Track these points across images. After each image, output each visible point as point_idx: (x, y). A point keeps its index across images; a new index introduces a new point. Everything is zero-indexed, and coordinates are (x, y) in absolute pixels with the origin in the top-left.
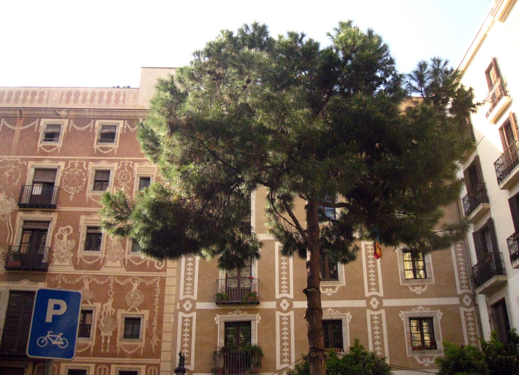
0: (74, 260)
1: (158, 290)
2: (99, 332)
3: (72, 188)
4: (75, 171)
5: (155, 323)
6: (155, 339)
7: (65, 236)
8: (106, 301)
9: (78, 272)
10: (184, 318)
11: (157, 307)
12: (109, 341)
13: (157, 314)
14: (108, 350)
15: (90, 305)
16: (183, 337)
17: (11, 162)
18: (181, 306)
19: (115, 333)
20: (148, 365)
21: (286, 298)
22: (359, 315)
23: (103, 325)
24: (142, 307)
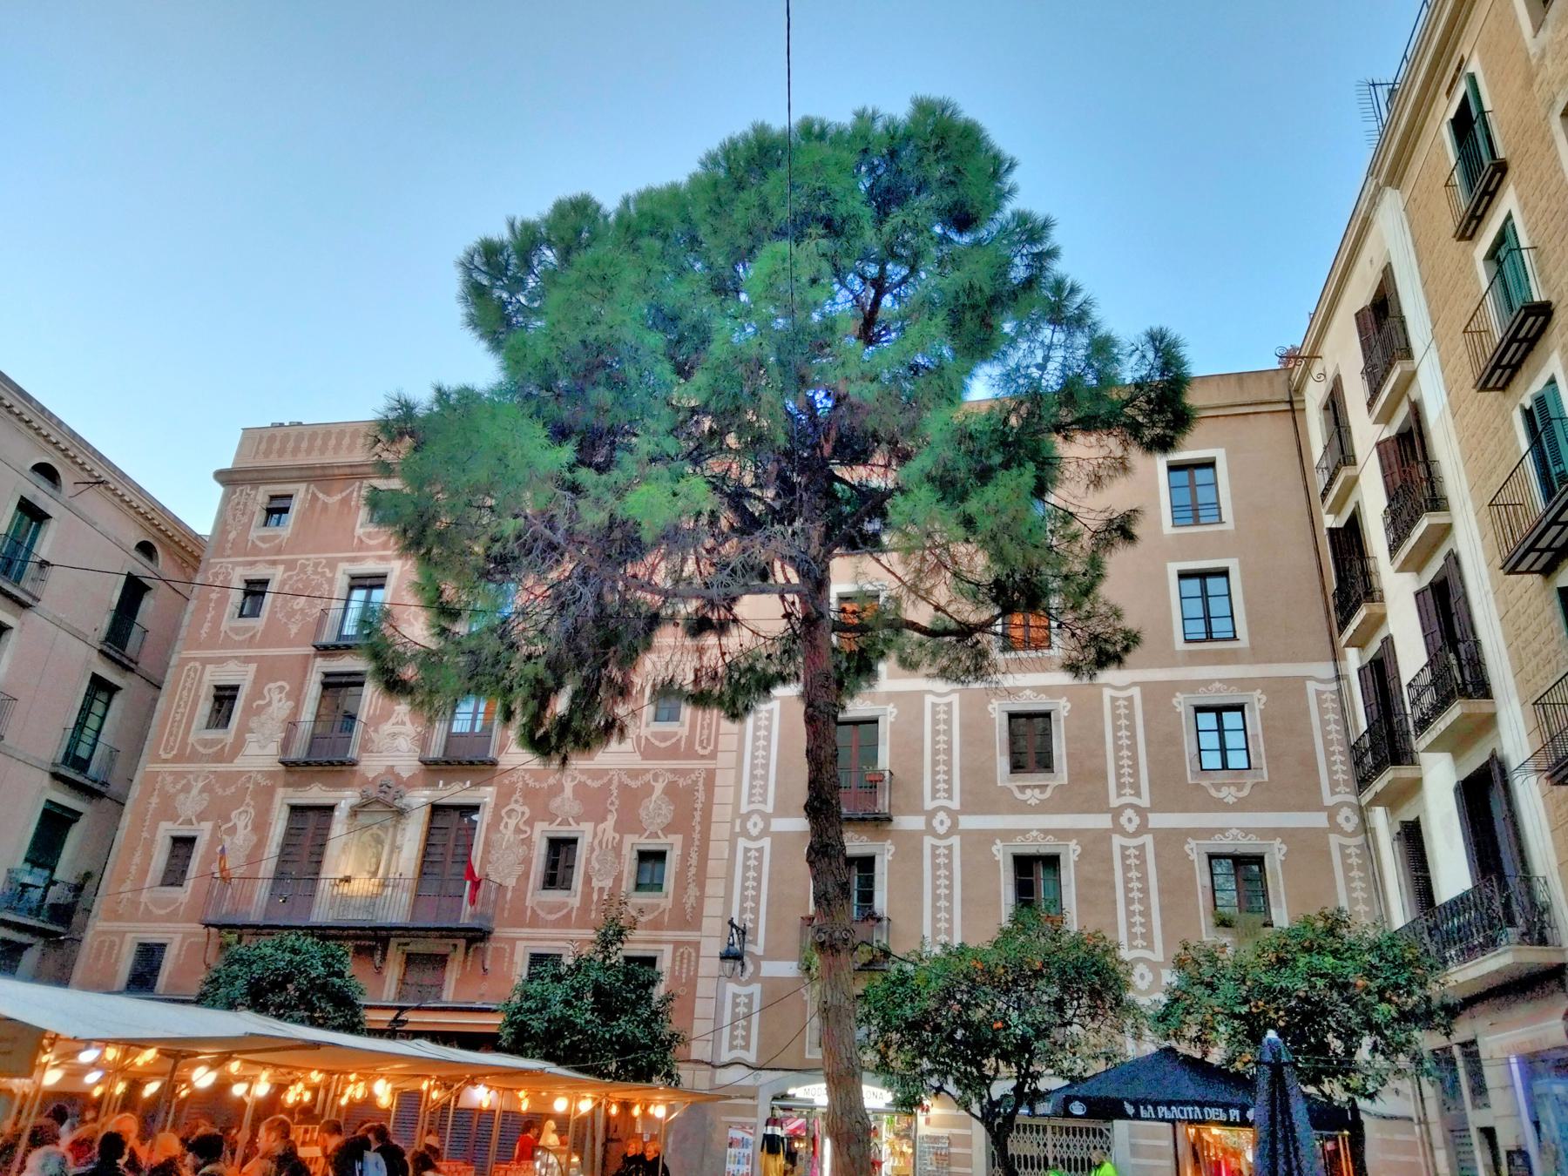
1: (701, 796)
2: (588, 880)
6: (693, 891)
8: (604, 819)
10: (747, 850)
11: (698, 828)
16: (744, 888)
19: (618, 880)
23: (597, 866)
24: (668, 829)
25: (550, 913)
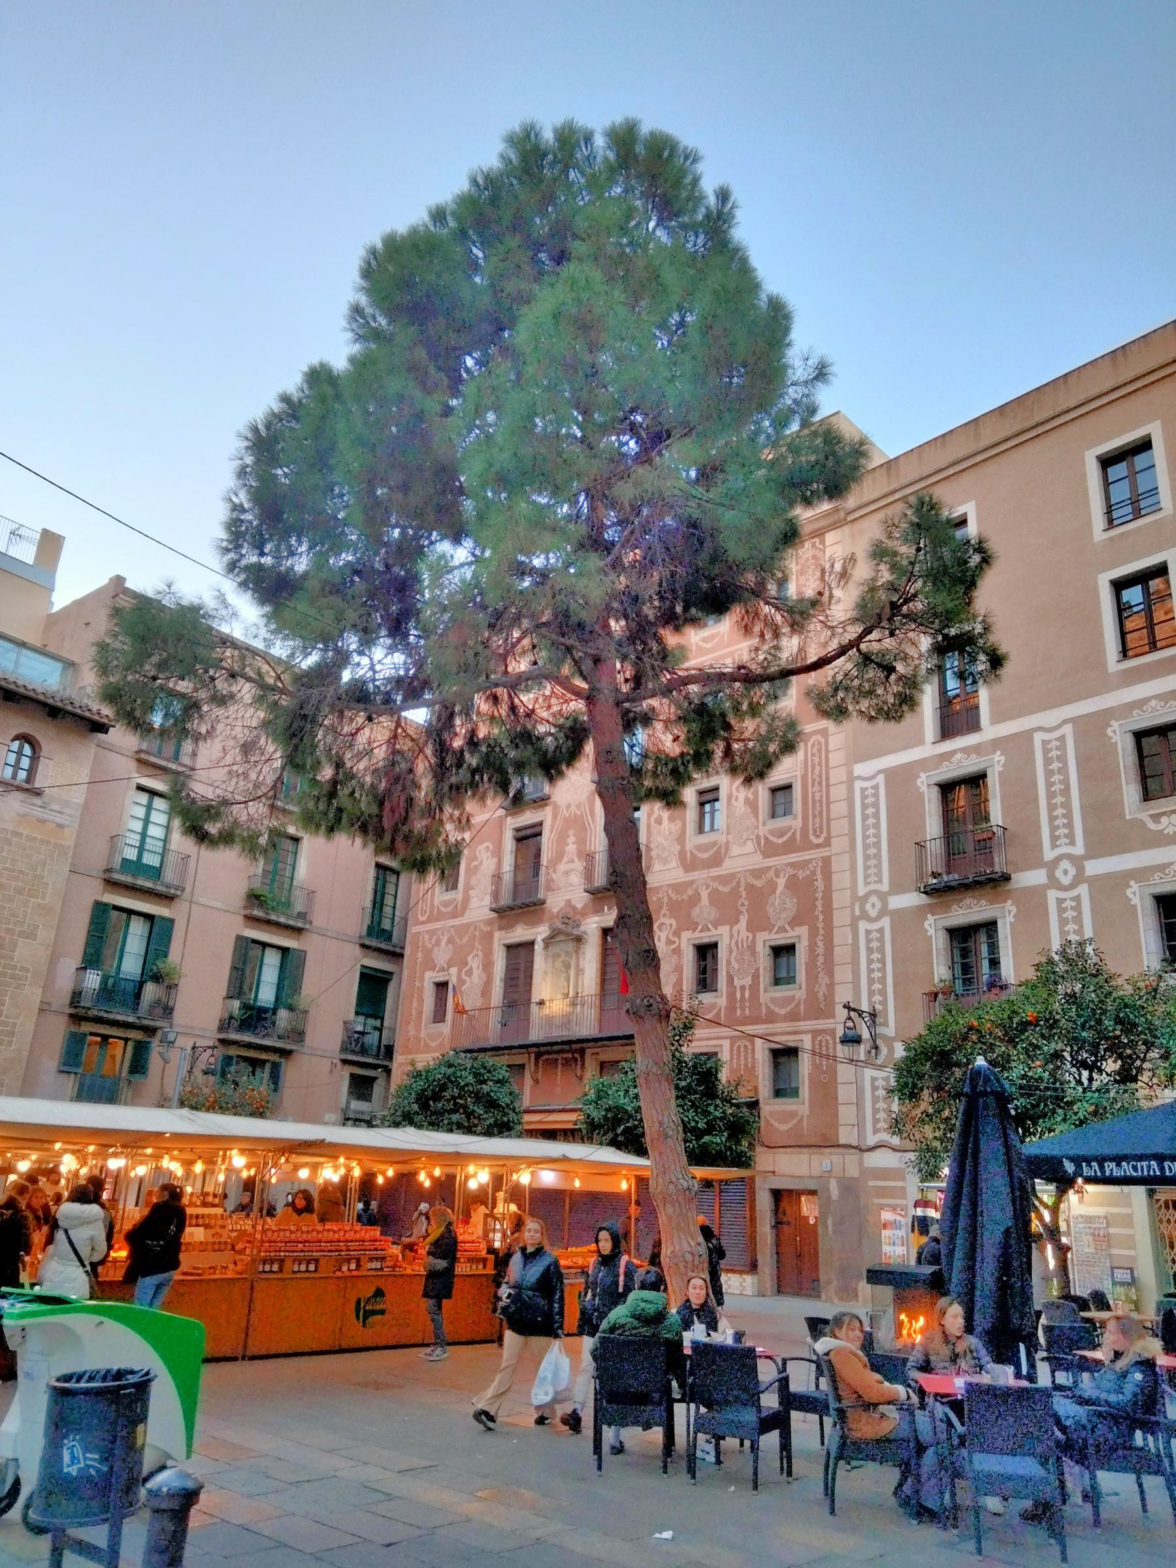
1: (820, 884)
5: (821, 949)
6: (823, 980)
8: (737, 921)
11: (821, 918)
12: (747, 995)
13: (822, 932)
14: (747, 1012)
16: (870, 971)
19: (756, 977)
24: (795, 922)
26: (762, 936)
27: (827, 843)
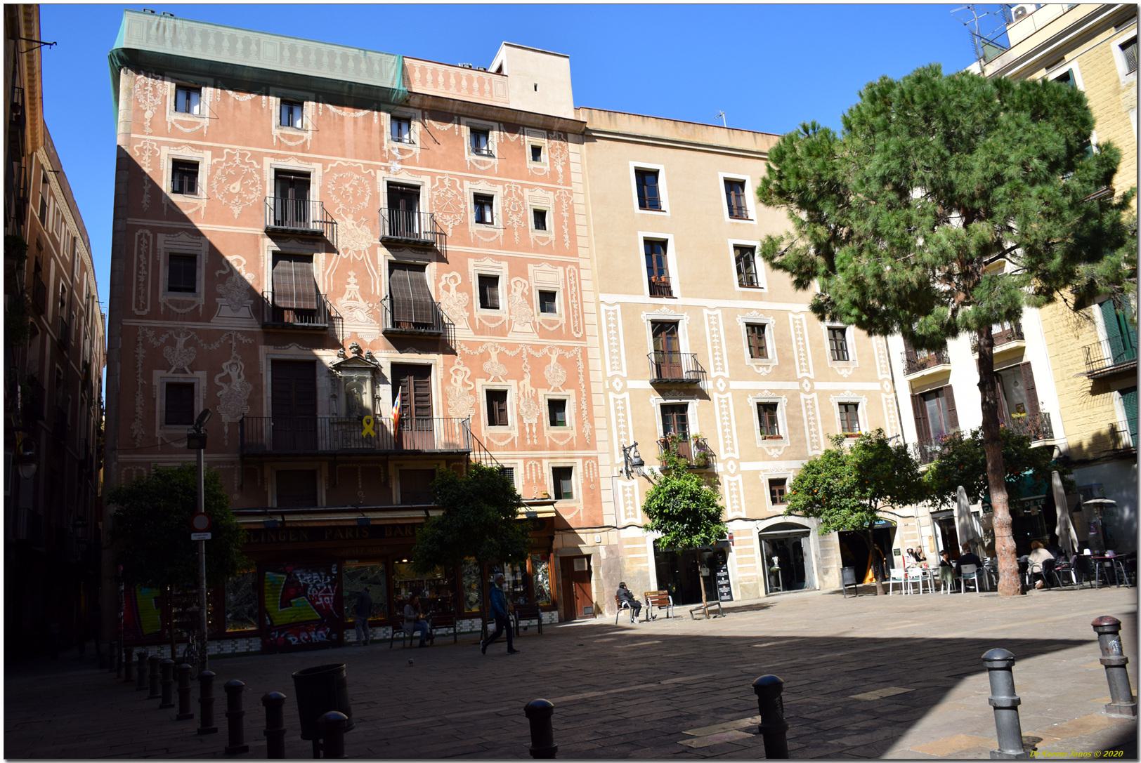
0: (471, 320)
1: (580, 363)
2: (520, 419)
3: (448, 217)
4: (446, 193)
6: (587, 426)
7: (453, 286)
9: (480, 338)
12: (534, 430)
15: (504, 383)
16: (618, 424)
17: (349, 168)
18: (610, 384)
20: (585, 458)
21: (722, 377)
22: (794, 395)
24: (565, 385)
25: (500, 440)
26: (542, 392)
27: (584, 338)
